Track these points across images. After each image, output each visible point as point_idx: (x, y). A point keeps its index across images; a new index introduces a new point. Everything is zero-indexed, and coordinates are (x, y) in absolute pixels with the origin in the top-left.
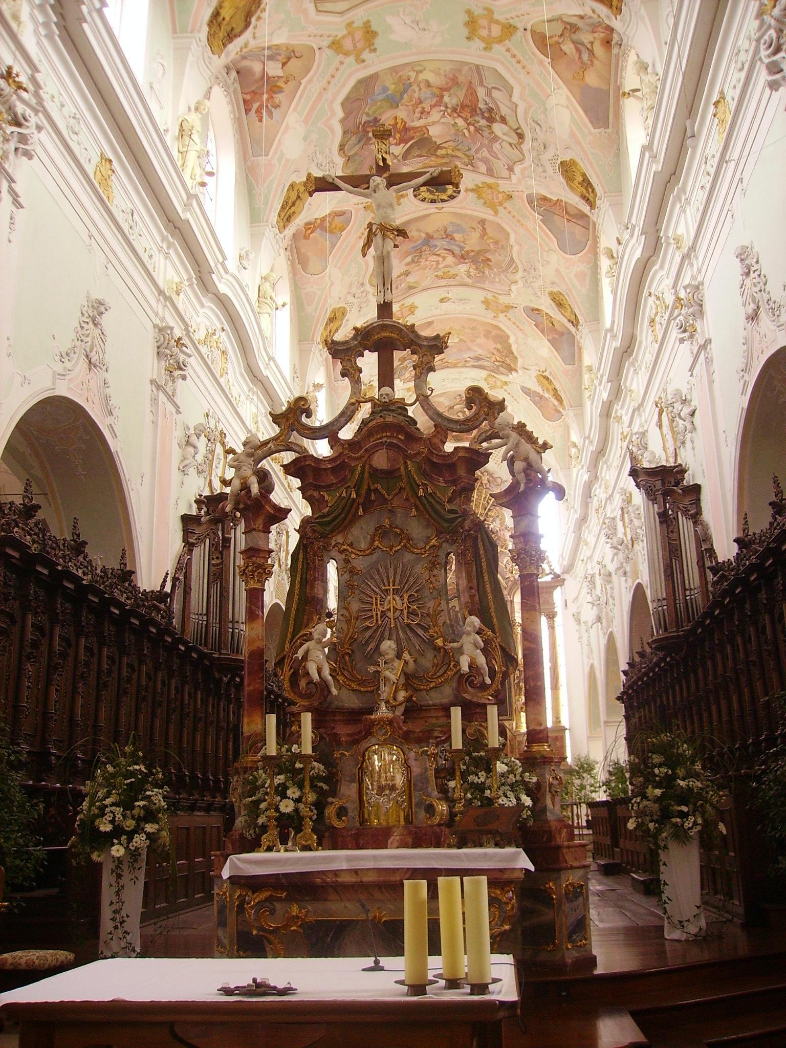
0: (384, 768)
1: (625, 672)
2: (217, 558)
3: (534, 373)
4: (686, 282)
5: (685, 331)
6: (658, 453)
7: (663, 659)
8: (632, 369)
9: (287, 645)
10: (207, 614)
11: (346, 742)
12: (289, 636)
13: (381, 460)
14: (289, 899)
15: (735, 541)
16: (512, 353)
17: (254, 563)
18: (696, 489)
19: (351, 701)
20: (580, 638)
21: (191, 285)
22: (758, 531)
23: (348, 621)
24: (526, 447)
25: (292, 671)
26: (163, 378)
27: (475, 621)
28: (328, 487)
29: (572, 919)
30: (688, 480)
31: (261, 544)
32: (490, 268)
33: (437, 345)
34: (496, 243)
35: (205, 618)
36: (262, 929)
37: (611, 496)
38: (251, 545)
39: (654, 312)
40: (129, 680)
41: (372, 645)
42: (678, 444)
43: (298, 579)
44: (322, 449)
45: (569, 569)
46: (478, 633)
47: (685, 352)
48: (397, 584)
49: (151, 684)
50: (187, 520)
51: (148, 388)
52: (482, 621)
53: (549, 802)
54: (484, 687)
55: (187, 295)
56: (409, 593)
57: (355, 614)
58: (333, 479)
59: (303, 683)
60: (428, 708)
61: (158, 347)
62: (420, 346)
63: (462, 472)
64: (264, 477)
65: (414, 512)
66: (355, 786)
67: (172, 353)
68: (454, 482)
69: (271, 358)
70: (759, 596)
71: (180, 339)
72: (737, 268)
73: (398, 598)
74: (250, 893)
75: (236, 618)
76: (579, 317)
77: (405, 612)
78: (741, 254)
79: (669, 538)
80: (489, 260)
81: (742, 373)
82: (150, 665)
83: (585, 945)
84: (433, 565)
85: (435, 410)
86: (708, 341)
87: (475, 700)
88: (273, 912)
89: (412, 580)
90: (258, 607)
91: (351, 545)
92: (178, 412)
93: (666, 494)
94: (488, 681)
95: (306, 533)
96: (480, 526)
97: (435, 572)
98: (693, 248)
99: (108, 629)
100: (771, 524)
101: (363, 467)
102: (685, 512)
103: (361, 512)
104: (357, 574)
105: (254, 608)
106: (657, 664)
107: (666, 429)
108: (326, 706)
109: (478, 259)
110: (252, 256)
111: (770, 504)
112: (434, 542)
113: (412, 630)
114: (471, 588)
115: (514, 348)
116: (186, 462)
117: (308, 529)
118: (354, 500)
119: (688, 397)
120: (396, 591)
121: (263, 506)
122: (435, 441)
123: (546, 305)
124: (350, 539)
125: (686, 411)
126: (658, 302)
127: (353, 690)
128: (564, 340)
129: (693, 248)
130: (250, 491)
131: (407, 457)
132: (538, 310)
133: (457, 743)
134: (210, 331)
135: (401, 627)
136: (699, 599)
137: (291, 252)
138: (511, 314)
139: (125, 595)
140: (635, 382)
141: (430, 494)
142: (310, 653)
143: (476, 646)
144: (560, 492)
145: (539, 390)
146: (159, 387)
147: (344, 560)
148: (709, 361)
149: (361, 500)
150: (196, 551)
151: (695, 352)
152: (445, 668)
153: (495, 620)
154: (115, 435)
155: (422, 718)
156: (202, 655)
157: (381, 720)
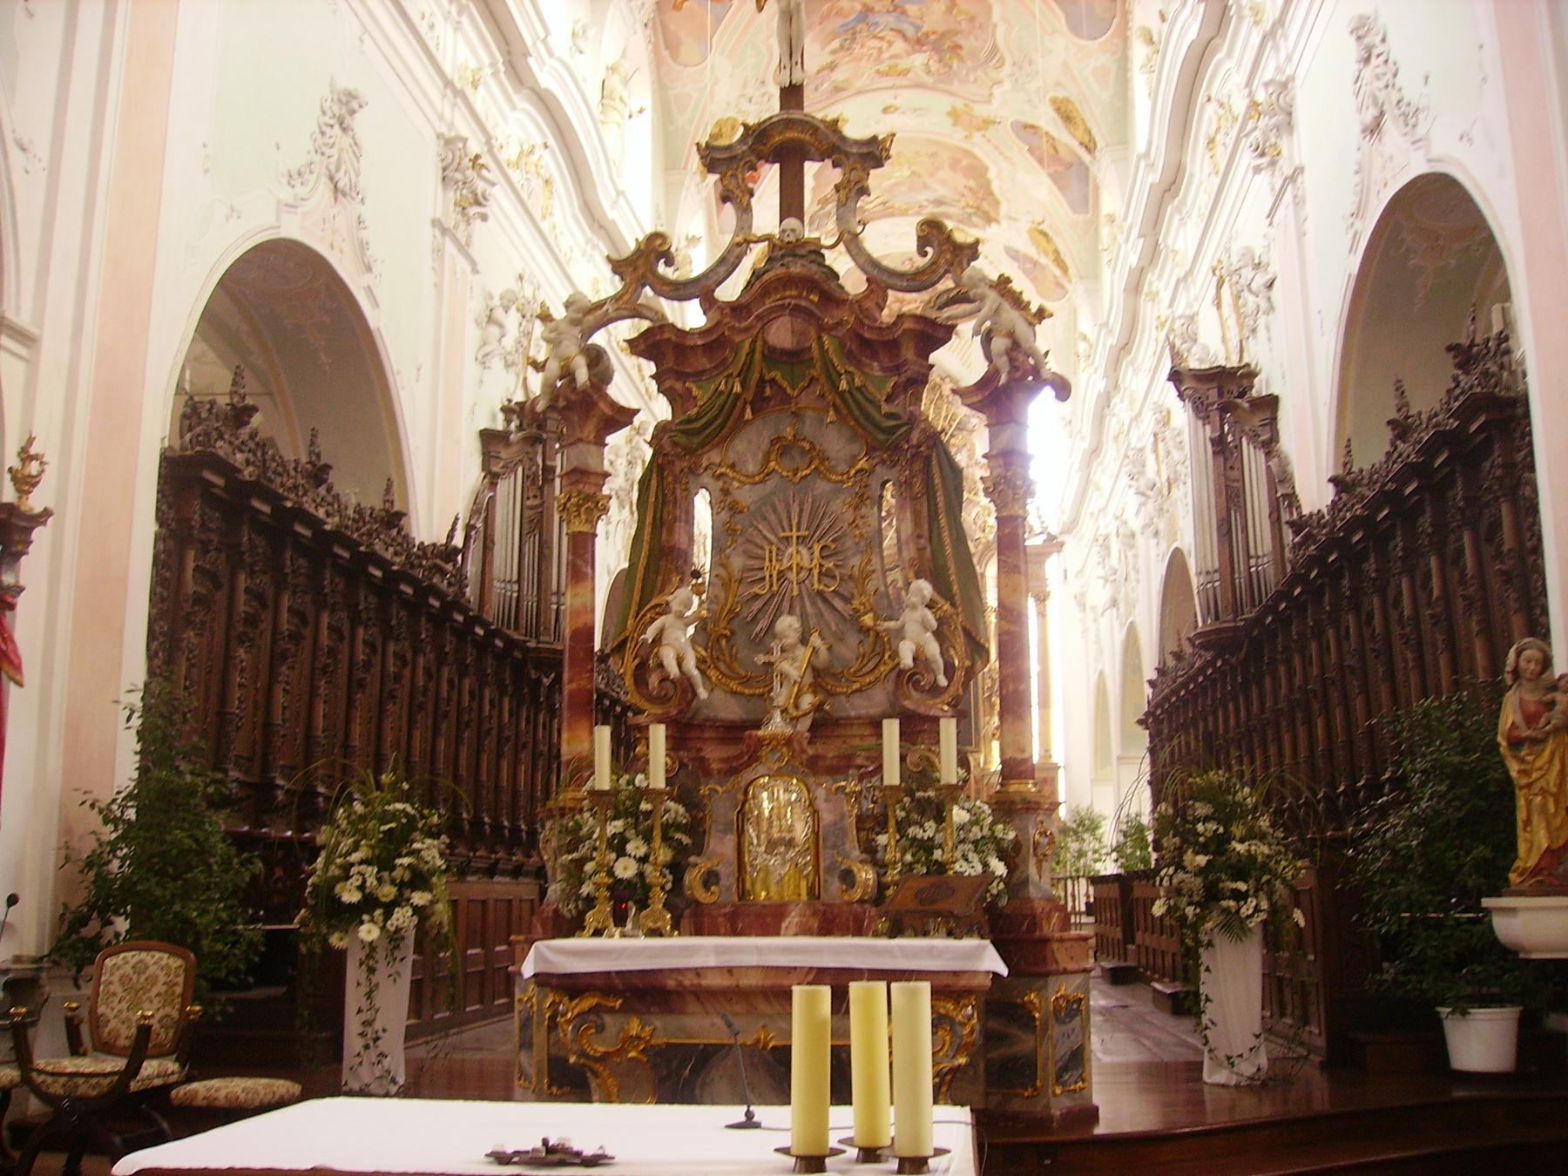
0: (778, 814)
1: (1152, 683)
3: (1025, 226)
4: (1268, 76)
5: (1262, 155)
6: (1213, 348)
7: (1211, 663)
8: (1177, 218)
10: (519, 581)
11: (719, 772)
13: (781, 334)
14: (626, 1010)
15: (1330, 480)
16: (991, 194)
17: (579, 493)
18: (1272, 402)
19: (729, 709)
20: (1085, 631)
21: (495, 74)
22: (1367, 467)
23: (726, 586)
24: (1011, 315)
26: (452, 218)
27: (925, 587)
28: (698, 375)
29: (1064, 1049)
30: (1260, 388)
31: (592, 464)
32: (961, 59)
33: (874, 153)
34: (972, 19)
35: (516, 587)
36: (583, 1054)
37: (1139, 414)
38: (575, 464)
39: (1214, 127)
40: (398, 678)
41: (763, 624)
42: (1246, 332)
43: (649, 520)
44: (690, 316)
45: (1070, 527)
46: (929, 606)
47: (1261, 188)
48: (804, 526)
49: (432, 685)
50: (487, 437)
51: (428, 228)
52: (936, 587)
53: (1032, 870)
54: (935, 690)
55: (488, 90)
56: (822, 543)
57: (737, 575)
58: (704, 363)
59: (654, 680)
60: (848, 722)
61: (444, 170)
62: (847, 155)
63: (908, 353)
64: (596, 358)
65: (831, 416)
66: (730, 840)
67: (464, 178)
68: (896, 369)
69: (619, 193)
70: (1365, 566)
71: (477, 157)
72: (1352, 50)
73: (804, 551)
74: (566, 999)
76: (1098, 139)
77: (816, 572)
78: (1357, 28)
79: (1227, 479)
80: (960, 47)
81: (1351, 220)
82: (432, 656)
83: (1081, 1089)
84: (861, 500)
85: (869, 256)
86: (1299, 170)
87: (922, 710)
88: (601, 1028)
89: (826, 524)
90: (586, 561)
91: (733, 466)
92: (475, 271)
93: (1223, 409)
94: (943, 681)
96: (934, 440)
97: (864, 510)
98: (1280, 22)
99: (366, 601)
100: (1389, 455)
101: (754, 342)
102: (1254, 436)
103: (748, 415)
104: (741, 512)
105: (579, 562)
106: (1202, 670)
107: (1227, 308)
108: (689, 715)
109: (942, 46)
110: (592, 32)
111: (1389, 423)
112: (861, 464)
113: (825, 600)
114: (919, 537)
115: (995, 186)
116: (487, 349)
118: (738, 396)
119: (1264, 261)
120: (801, 540)
121: (594, 404)
122: (869, 304)
123: (1046, 119)
124: (732, 457)
125: (1260, 280)
126: (1221, 112)
127: (734, 693)
128: (1072, 176)
129: (1280, 22)
131: (822, 328)
132: (1032, 127)
133: (892, 776)
134: (526, 147)
135: (809, 596)
136: (1271, 572)
137: (654, 30)
138: (991, 131)
140: (1181, 237)
141: (859, 389)
142: (666, 633)
143: (924, 625)
144: (1063, 389)
145: (1031, 251)
146: (445, 231)
147: (721, 490)
148: (1299, 202)
149: (749, 396)
150: (503, 487)
151: (1277, 187)
152: (876, 660)
153: (955, 588)
154: (375, 303)
155: (838, 737)
156: (511, 643)
157: (774, 737)
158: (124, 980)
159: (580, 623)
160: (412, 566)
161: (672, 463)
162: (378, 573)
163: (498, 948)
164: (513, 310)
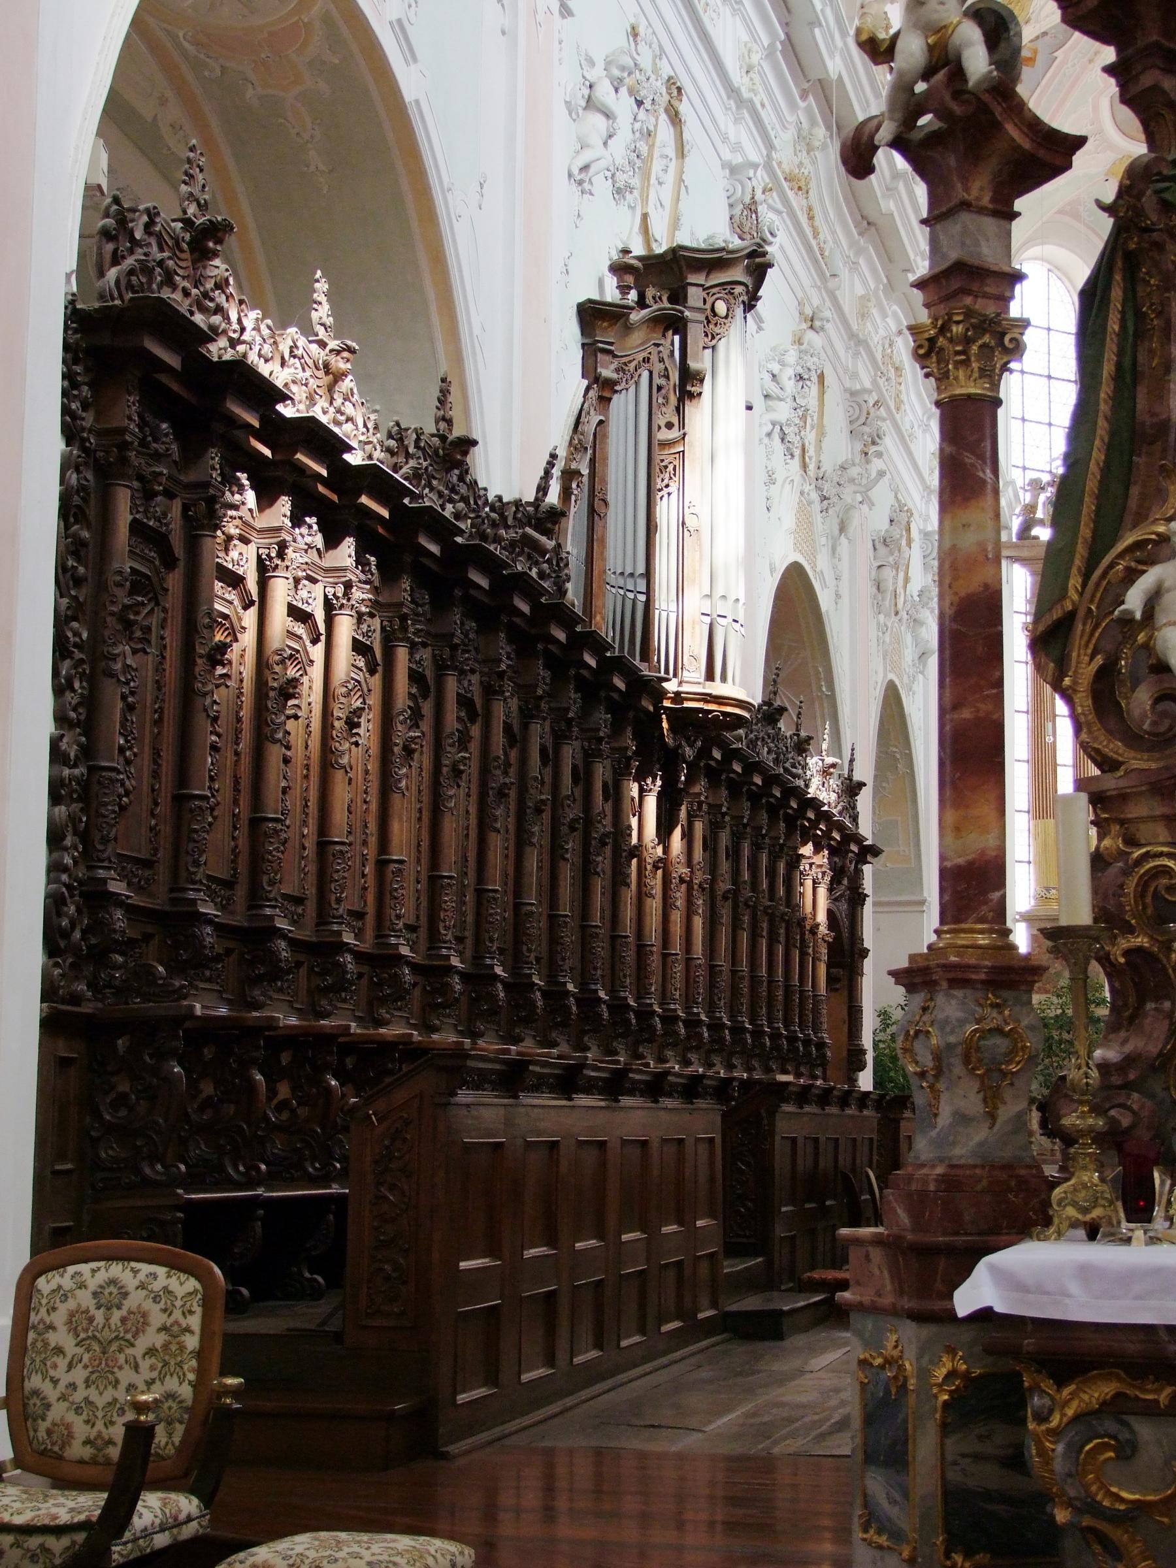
2: (669, 426)
9: (1075, 581)
12: (1081, 551)
17: (969, 313)
25: (1099, 660)
31: (988, 255)
36: (1091, 1507)
38: (953, 256)
40: (463, 742)
43: (1108, 369)
49: (514, 754)
50: (592, 315)
59: (1140, 701)
74: (1048, 1385)
75: (720, 591)
82: (514, 704)
88: (1127, 1450)
90: (981, 457)
95: (1139, 212)
105: (969, 459)
117: (1149, 201)
121: (997, 126)
130: (958, 73)
139: (449, 507)
150: (621, 403)
154: (411, 55)
158: (78, 1322)
159: (972, 584)
160: (483, 537)
161: (1159, 247)
162: (434, 549)
163: (665, 1230)
164: (624, 90)
